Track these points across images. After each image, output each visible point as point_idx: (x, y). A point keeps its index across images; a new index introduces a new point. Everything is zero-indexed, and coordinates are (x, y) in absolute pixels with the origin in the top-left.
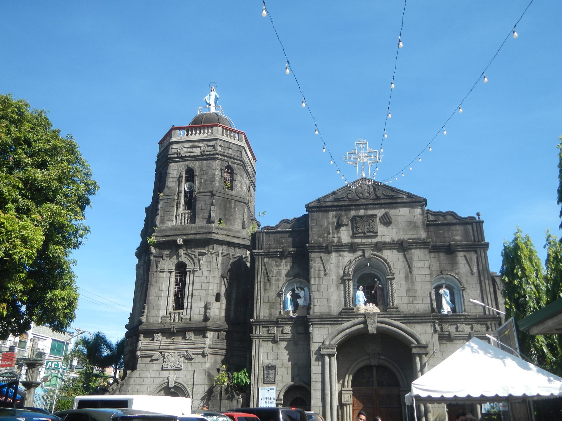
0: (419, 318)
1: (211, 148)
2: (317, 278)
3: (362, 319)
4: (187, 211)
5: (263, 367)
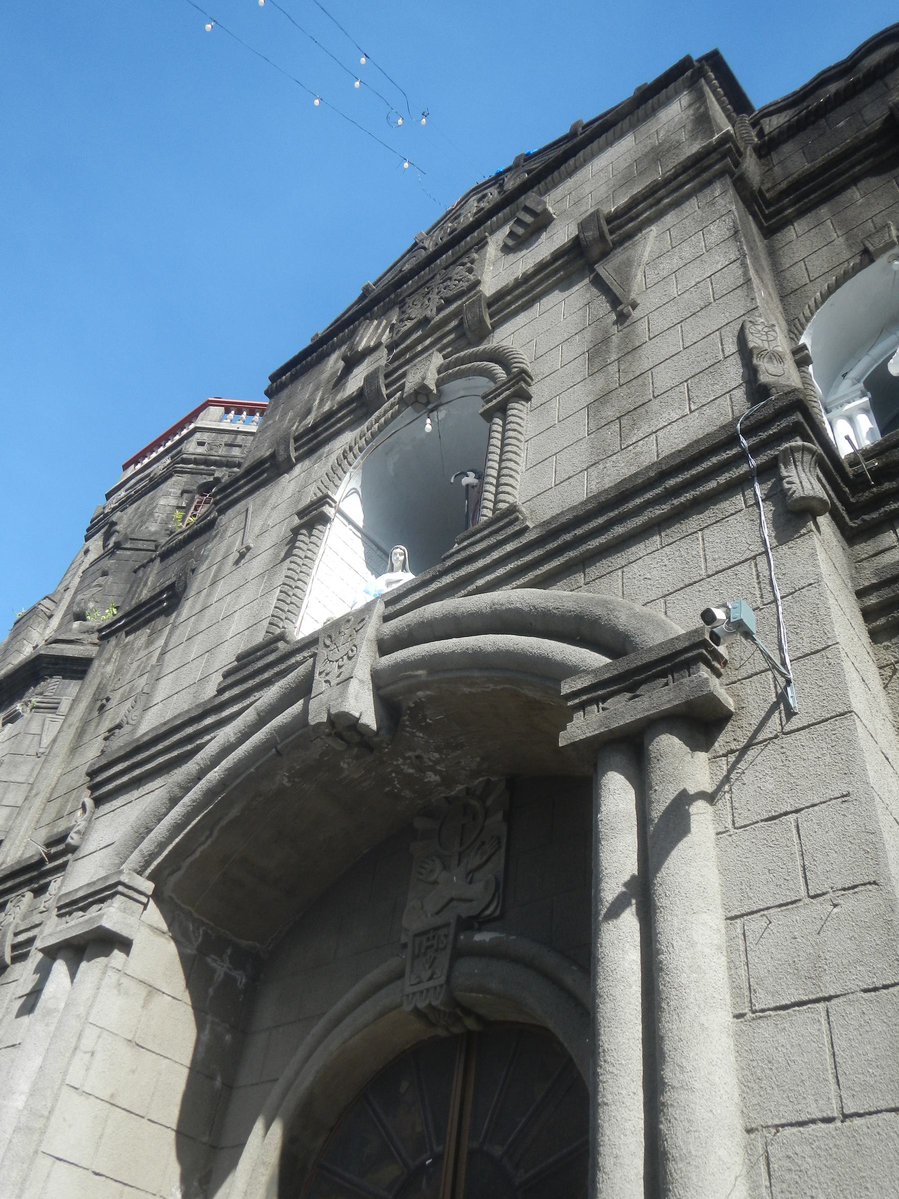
0: (649, 495)
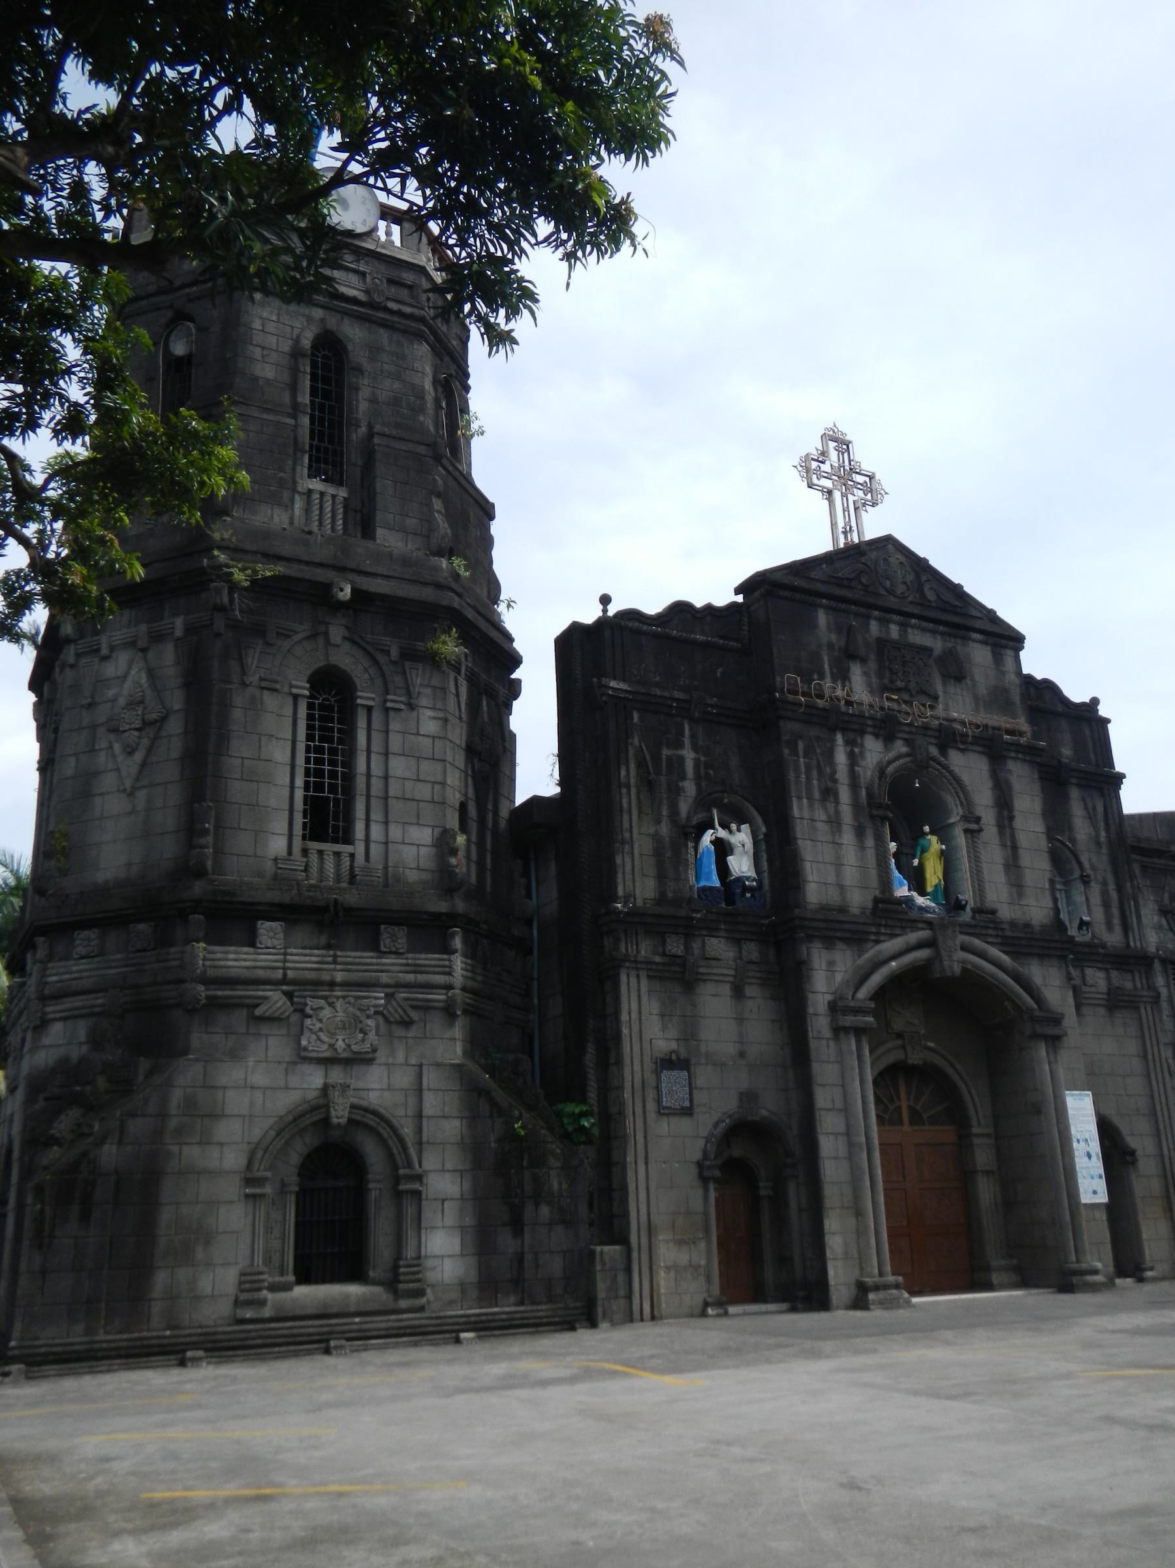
1: (404, 294)
2: (805, 801)
3: (924, 934)
4: (330, 490)
5: (656, 1063)
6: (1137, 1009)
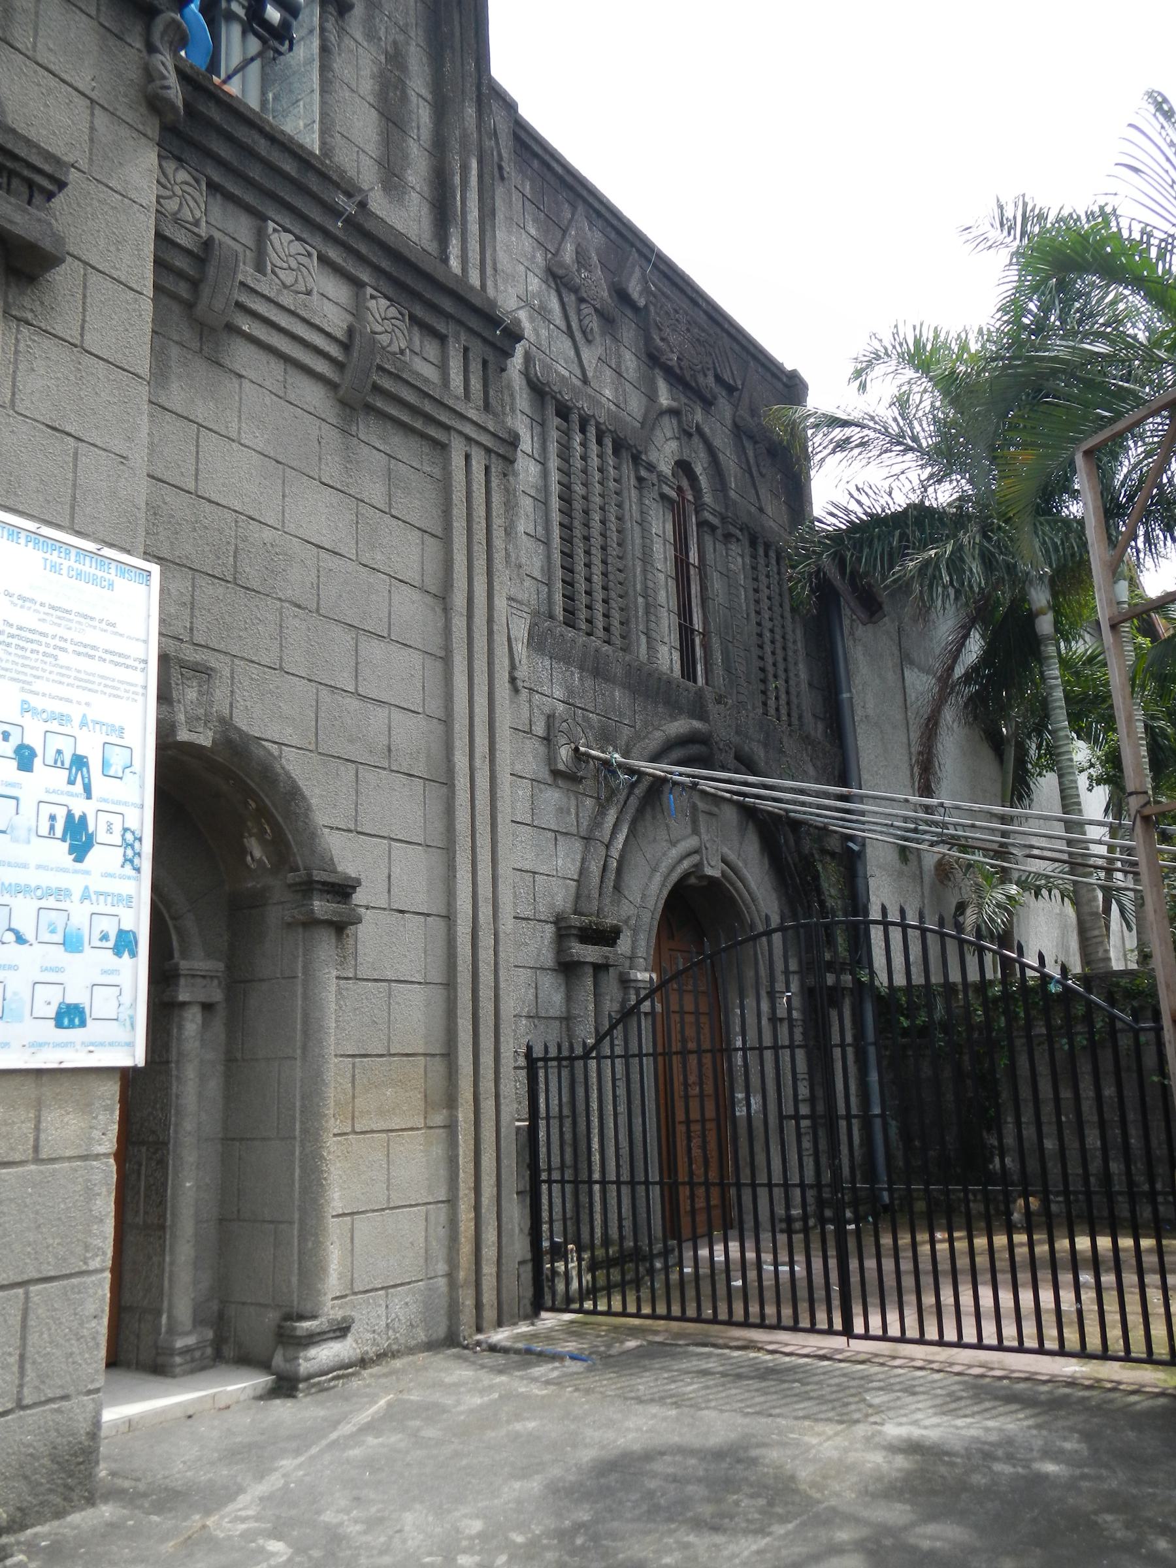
6: (442, 447)
